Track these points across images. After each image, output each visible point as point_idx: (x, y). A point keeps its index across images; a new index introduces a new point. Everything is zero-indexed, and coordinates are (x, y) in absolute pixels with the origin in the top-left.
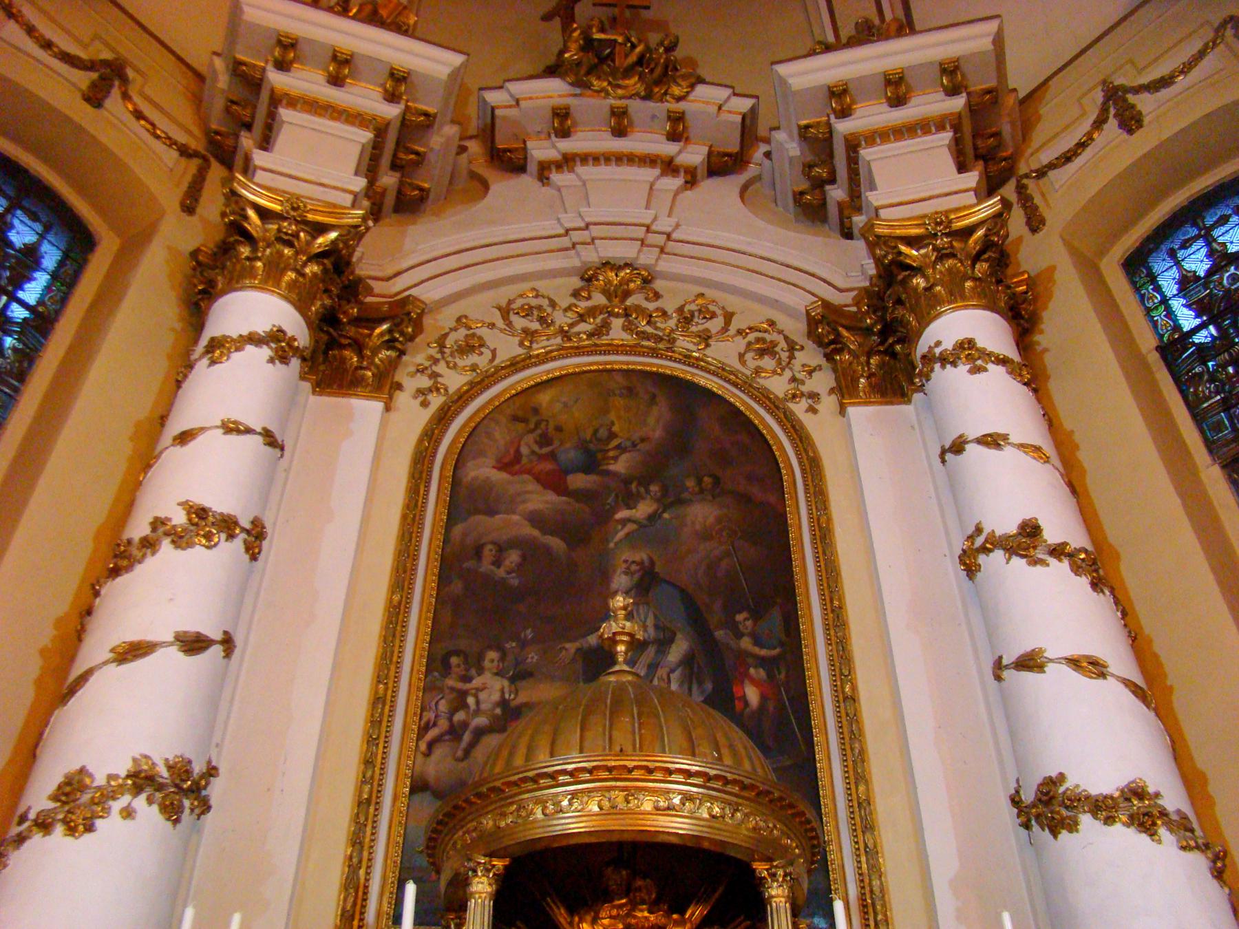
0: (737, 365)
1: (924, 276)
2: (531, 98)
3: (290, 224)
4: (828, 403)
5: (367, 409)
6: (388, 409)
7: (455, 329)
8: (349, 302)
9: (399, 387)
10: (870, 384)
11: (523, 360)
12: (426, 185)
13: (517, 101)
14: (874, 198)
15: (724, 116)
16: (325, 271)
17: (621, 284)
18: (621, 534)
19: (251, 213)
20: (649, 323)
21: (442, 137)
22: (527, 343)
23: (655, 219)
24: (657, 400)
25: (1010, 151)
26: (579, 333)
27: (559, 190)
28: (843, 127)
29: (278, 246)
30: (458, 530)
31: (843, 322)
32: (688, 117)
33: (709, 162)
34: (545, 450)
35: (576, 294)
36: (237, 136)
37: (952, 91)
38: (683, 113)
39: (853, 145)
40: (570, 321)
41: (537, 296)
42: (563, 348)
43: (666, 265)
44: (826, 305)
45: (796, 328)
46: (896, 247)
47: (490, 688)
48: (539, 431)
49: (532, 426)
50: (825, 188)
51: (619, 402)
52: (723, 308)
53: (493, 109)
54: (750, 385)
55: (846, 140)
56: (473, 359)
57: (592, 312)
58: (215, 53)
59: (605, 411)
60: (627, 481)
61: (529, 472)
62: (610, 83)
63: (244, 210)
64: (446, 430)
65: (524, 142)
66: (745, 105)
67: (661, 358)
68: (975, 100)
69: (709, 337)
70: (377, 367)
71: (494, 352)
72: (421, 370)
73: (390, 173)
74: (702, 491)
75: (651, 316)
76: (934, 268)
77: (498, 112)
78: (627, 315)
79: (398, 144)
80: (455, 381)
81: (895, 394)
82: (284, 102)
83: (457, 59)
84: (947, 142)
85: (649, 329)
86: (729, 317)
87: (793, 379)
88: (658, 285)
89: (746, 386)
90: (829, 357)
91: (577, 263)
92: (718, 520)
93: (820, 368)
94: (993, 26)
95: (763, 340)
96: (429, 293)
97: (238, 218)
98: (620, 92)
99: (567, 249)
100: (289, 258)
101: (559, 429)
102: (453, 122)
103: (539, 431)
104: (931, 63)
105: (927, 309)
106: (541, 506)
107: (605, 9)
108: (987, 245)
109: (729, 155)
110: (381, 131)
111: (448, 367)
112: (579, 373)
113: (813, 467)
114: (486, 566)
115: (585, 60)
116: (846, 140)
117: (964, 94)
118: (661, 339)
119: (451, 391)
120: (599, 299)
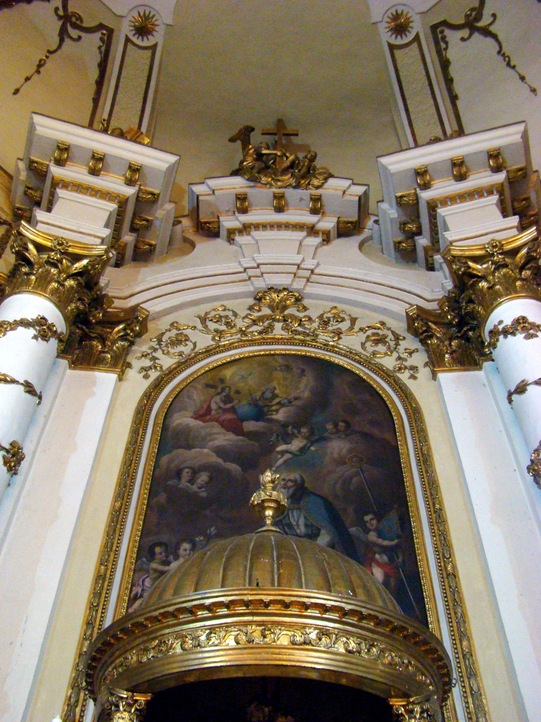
0: (359, 349)
1: (486, 281)
2: (221, 189)
3: (56, 254)
4: (424, 373)
5: (105, 379)
6: (120, 379)
7: (170, 331)
8: (97, 309)
9: (129, 365)
10: (453, 358)
11: (215, 348)
12: (153, 243)
13: (213, 191)
14: (450, 236)
15: (347, 197)
16: (79, 284)
17: (281, 301)
18: (281, 461)
19: (31, 246)
20: (299, 325)
21: (163, 212)
22: (217, 338)
23: (303, 260)
24: (306, 373)
25: (536, 211)
26: (252, 332)
27: (241, 247)
28: (425, 195)
29: (47, 267)
30: (165, 459)
31: (432, 319)
32: (323, 198)
33: (338, 228)
34: (229, 406)
35: (251, 308)
36: (31, 211)
37: (497, 169)
38: (321, 196)
39: (432, 207)
40: (246, 325)
41: (225, 310)
42: (241, 341)
43: (310, 289)
44: (419, 308)
45: (400, 327)
46: (466, 263)
48: (224, 394)
49: (219, 390)
50: (415, 237)
51: (279, 374)
52: (350, 315)
53: (198, 197)
54: (370, 362)
55: (428, 203)
56: (181, 348)
57: (261, 319)
58: (18, 159)
59: (270, 380)
60: (285, 425)
61: (217, 421)
62: (273, 179)
63: (26, 244)
64: (160, 393)
65: (218, 217)
66: (360, 190)
67: (308, 346)
68: (512, 175)
69: (341, 333)
70: (115, 352)
71: (195, 344)
72: (144, 355)
73: (129, 233)
74: (338, 431)
75: (301, 320)
76: (494, 276)
77: (201, 198)
78: (285, 321)
79: (134, 214)
80: (167, 362)
81: (470, 365)
82: (60, 185)
83: (173, 159)
84: (495, 201)
85: (300, 329)
86: (353, 321)
87: (399, 358)
88: (306, 302)
89: (367, 363)
90: (423, 342)
91: (252, 289)
92: (350, 451)
93: (417, 350)
94: (520, 128)
95: (377, 334)
96: (153, 307)
97: (21, 249)
98: (279, 184)
99: (245, 281)
100: (55, 275)
101: (238, 392)
102: (170, 201)
103: (224, 394)
104: (481, 152)
105: (491, 301)
106: (224, 443)
107: (268, 136)
108: (530, 259)
109: (351, 223)
110: (123, 203)
111: (163, 353)
112: (252, 357)
113: (415, 414)
114: (184, 483)
115: (256, 165)
116: (428, 203)
117: (505, 172)
118: (308, 335)
119: (164, 368)
120: (266, 311)
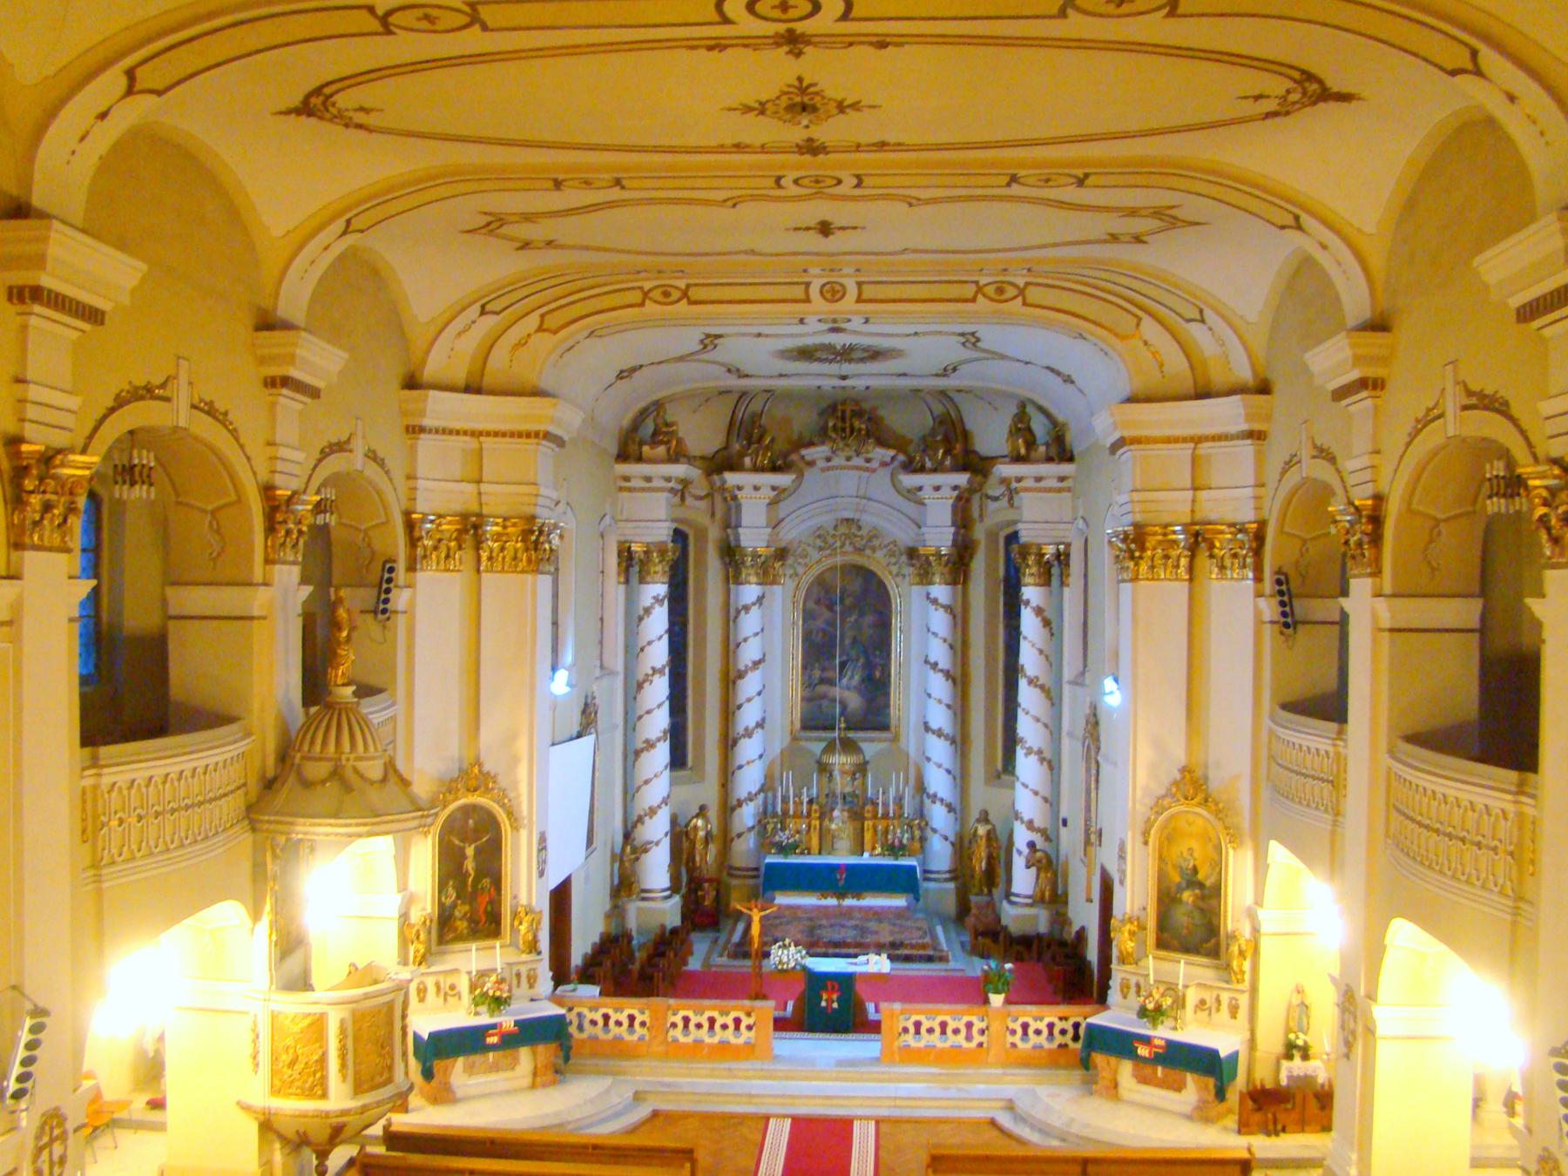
5: (777, 589)
47: (817, 674)
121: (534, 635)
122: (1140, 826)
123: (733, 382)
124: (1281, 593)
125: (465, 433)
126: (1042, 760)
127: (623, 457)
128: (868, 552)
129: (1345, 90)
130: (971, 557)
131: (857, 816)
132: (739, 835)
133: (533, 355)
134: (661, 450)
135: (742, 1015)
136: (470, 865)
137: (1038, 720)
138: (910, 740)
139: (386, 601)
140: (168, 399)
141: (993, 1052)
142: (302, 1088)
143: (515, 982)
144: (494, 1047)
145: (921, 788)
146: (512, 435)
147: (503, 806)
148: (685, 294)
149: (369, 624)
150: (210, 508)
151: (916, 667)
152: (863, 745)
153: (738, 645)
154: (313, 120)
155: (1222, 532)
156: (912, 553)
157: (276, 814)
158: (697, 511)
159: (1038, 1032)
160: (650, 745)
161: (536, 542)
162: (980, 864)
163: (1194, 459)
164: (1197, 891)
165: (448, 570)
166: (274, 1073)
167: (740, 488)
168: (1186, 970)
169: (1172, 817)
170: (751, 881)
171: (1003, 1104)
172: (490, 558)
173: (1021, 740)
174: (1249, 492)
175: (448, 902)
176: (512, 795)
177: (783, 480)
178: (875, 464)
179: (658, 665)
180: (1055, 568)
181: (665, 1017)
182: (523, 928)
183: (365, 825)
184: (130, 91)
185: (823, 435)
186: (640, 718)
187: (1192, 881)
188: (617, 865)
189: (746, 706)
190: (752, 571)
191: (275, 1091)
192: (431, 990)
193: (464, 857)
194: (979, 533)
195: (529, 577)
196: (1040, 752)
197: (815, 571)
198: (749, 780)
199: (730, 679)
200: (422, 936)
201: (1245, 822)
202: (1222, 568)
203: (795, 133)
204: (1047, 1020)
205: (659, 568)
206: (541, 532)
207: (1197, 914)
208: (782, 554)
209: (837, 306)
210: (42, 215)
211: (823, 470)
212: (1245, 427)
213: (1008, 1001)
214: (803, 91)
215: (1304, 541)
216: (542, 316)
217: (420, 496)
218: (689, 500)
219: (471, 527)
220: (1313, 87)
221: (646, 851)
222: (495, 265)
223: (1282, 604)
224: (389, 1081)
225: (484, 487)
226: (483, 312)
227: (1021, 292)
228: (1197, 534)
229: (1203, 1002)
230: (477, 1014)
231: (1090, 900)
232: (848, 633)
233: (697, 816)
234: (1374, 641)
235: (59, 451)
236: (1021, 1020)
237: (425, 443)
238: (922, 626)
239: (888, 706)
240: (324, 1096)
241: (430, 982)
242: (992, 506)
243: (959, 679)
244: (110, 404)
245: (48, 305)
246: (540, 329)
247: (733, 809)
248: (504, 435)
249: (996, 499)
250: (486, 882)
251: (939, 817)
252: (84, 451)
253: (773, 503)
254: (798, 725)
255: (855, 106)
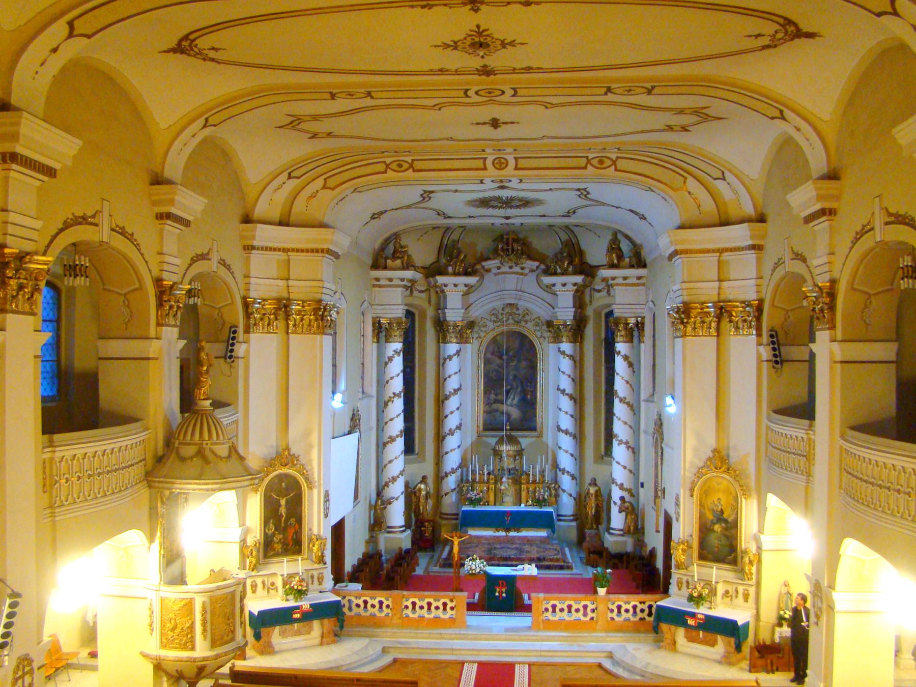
47: (493, 396)
121: (321, 372)
122: (688, 486)
123: (441, 221)
124: (773, 343)
125: (279, 250)
126: (628, 447)
127: (375, 266)
128: (523, 323)
129: (811, 30)
130: (585, 327)
131: (517, 482)
132: (446, 494)
133: (321, 204)
134: (398, 262)
135: (447, 601)
136: (283, 510)
137: (626, 423)
138: (549, 437)
139: (232, 351)
140: (96, 225)
141: (600, 623)
142: (180, 645)
143: (310, 581)
144: (297, 620)
145: (555, 465)
146: (307, 251)
147: (303, 474)
148: (411, 166)
149: (222, 364)
150: (123, 292)
151: (552, 391)
152: (521, 440)
153: (445, 380)
154: (184, 56)
155: (737, 307)
156: (549, 324)
157: (164, 477)
158: (420, 300)
159: (627, 611)
160: (392, 439)
161: (322, 316)
162: (591, 511)
163: (719, 262)
164: (723, 525)
165: (270, 333)
166: (162, 634)
167: (446, 285)
168: (716, 573)
169: (707, 480)
170: (454, 522)
171: (605, 654)
172: (294, 325)
173: (616, 436)
174: (753, 282)
175: (270, 533)
176: (308, 468)
177: (472, 280)
178: (527, 271)
179: (397, 392)
180: (635, 331)
181: (401, 603)
182: (315, 549)
183: (217, 483)
184: (71, 35)
185: (496, 253)
186: (386, 423)
187: (720, 517)
188: (372, 512)
189: (450, 416)
190: (453, 335)
191: (163, 646)
192: (260, 585)
193: (280, 505)
194: (589, 312)
195: (318, 337)
196: (627, 443)
197: (490, 336)
198: (452, 460)
199: (441, 400)
200: (254, 553)
201: (752, 484)
202: (737, 328)
203: (474, 62)
204: (633, 603)
205: (397, 333)
206: (325, 309)
207: (723, 539)
208: (471, 325)
209: (503, 172)
210: (17, 109)
211: (496, 274)
212: (750, 242)
213: (608, 592)
214: (480, 34)
215: (787, 311)
216: (325, 180)
217: (252, 287)
218: (415, 293)
219: (283, 307)
220: (791, 29)
221: (390, 503)
222: (297, 148)
223: (774, 349)
224: (233, 639)
225: (291, 283)
226: (290, 177)
227: (614, 163)
228: (721, 308)
229: (727, 592)
230: (287, 600)
231: (658, 531)
232: (511, 374)
233: (421, 483)
234: (831, 368)
235: (28, 254)
236: (616, 604)
237: (255, 255)
238: (556, 368)
239: (536, 416)
240: (193, 648)
241: (259, 581)
242: (597, 295)
243: (578, 400)
244: (61, 226)
245: (21, 164)
246: (324, 187)
247: (442, 478)
248: (302, 251)
249: (599, 291)
250: (292, 521)
251: (566, 482)
252: (44, 254)
253: (466, 294)
254: (481, 428)
255: (512, 43)
